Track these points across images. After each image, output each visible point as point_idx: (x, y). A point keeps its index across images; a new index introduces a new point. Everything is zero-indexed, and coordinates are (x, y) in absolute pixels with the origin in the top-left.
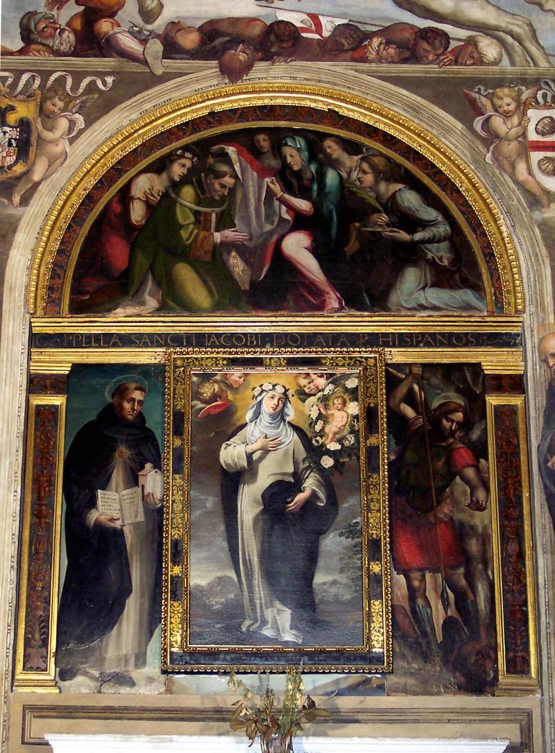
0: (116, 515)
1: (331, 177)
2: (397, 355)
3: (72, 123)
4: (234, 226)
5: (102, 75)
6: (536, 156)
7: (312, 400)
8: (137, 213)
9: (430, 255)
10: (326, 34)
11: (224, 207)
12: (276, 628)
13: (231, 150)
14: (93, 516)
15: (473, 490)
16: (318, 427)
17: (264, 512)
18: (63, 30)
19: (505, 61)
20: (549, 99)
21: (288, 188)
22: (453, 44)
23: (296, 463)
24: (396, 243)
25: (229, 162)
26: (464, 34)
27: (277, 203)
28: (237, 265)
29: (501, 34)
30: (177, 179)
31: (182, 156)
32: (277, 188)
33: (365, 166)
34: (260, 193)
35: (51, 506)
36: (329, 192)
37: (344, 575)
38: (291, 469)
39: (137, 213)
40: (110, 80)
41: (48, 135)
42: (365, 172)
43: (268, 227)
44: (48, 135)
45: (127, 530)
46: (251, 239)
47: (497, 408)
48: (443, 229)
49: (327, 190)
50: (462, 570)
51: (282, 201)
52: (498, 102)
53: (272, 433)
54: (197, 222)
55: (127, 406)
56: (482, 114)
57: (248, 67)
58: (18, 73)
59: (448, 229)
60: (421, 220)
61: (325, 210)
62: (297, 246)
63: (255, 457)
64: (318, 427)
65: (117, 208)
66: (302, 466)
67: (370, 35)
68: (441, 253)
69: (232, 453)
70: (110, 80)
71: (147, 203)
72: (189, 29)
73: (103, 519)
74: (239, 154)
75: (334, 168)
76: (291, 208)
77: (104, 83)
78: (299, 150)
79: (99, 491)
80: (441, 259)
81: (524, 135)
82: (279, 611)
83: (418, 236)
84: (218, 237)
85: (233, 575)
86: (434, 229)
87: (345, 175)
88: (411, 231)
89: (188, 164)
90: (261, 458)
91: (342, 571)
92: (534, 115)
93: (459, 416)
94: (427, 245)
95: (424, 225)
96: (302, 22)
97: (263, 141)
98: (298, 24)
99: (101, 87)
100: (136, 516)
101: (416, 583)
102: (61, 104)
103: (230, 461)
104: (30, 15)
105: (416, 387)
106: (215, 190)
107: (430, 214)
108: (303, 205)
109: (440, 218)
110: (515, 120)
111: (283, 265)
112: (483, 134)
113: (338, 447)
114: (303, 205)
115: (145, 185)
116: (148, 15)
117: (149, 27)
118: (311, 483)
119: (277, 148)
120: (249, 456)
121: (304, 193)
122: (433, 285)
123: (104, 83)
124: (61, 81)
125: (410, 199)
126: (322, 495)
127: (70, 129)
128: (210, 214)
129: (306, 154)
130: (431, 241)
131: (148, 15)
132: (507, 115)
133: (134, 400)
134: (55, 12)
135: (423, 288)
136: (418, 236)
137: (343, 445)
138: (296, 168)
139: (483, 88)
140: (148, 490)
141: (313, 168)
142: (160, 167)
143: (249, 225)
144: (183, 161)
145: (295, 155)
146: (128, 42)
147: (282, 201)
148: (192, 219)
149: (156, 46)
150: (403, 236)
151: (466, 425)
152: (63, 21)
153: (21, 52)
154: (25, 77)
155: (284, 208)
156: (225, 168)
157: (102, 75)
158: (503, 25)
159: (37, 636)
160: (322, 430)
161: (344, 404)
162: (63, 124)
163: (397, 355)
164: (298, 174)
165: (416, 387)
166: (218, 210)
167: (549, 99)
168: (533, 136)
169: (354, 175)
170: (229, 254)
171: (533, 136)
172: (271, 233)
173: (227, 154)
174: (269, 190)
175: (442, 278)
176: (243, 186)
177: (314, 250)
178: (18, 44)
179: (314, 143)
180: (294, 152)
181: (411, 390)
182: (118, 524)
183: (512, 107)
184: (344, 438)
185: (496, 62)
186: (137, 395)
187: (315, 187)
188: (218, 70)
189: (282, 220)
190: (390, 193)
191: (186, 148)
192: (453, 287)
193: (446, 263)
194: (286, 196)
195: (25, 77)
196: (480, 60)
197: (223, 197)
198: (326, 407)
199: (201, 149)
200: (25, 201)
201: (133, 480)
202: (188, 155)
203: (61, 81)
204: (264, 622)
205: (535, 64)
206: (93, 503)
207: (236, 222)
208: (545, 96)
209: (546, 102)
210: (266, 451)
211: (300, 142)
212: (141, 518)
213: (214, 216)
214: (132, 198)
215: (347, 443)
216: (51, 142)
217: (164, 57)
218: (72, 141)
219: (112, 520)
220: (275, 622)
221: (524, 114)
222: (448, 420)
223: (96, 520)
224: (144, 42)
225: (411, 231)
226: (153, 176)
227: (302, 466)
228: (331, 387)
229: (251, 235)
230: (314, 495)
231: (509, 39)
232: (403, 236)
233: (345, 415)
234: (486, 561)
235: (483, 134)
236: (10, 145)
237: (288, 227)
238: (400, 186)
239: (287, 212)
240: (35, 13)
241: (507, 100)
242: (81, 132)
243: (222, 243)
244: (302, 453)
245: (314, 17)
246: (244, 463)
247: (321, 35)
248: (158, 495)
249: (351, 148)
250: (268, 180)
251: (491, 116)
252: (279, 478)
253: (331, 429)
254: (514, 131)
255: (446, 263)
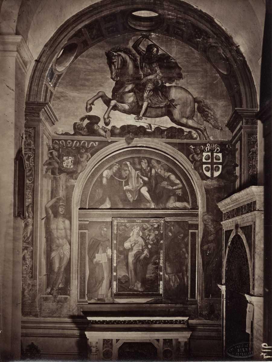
0: (100, 260)
1: (153, 171)
2: (168, 219)
3: (88, 156)
4: (129, 185)
5: (95, 141)
6: (204, 166)
7: (146, 231)
8: (105, 181)
9: (177, 193)
10: (153, 130)
11: (126, 179)
12: (137, 287)
13: (128, 163)
14: (95, 260)
15: (185, 254)
16: (148, 238)
17: (134, 259)
18: (84, 128)
19: (198, 139)
20: (209, 150)
21: (142, 174)
22: (185, 133)
23: (142, 247)
24: (169, 190)
25: (128, 167)
26: (188, 130)
27: (139, 178)
28: (129, 196)
29: (198, 130)
30: (114, 171)
31: (116, 165)
32: (140, 174)
33: (162, 168)
34: (135, 176)
35: (85, 258)
36: (153, 176)
37: (153, 274)
38: (141, 248)
39: (105, 181)
40: (97, 143)
41: (82, 160)
42: (162, 170)
43: (137, 185)
44: (82, 160)
45: (103, 264)
46: (133, 189)
47: (192, 233)
48: (180, 186)
49: (152, 175)
50: (181, 274)
51: (141, 178)
52: (196, 150)
53: (136, 239)
54: (119, 184)
55: (103, 232)
56: (192, 154)
57: (133, 139)
58: (73, 141)
59: (182, 185)
60: (176, 183)
61: (151, 181)
62: (144, 191)
63: (133, 245)
64: (148, 238)
65: (99, 179)
66: (144, 247)
67: (164, 131)
68: (179, 192)
69: (127, 245)
70: (97, 143)
71: (107, 178)
72: (118, 129)
73: (97, 261)
74: (131, 164)
75: (154, 168)
76: (143, 180)
77: (96, 144)
78: (145, 163)
79: (96, 254)
80: (179, 194)
81: (202, 160)
82: (138, 283)
83: (174, 188)
84: (125, 188)
85: (128, 275)
86: (178, 186)
87: (157, 170)
88: (173, 186)
89: (117, 167)
90: (134, 246)
91: (153, 273)
92: (205, 154)
93: (182, 235)
94: (177, 190)
95: (176, 184)
96: (147, 126)
97: (137, 160)
98: (146, 127)
99: (95, 145)
100: (105, 260)
101: (171, 277)
102: (84, 150)
103: (126, 246)
104: (75, 124)
105: (172, 228)
106: (124, 175)
107: (178, 181)
108: (146, 179)
109: (180, 183)
110: (200, 156)
111: (140, 195)
112: (191, 160)
113: (152, 242)
114: (146, 179)
115: (106, 173)
116: (107, 124)
117: (107, 127)
118: (146, 252)
119: (140, 164)
120: (131, 245)
121: (147, 176)
122: (177, 201)
123: (96, 144)
124: (84, 143)
125: (173, 177)
126: (148, 255)
127: (87, 158)
128: (123, 182)
129: (147, 164)
130: (177, 189)
131: (107, 124)
132: (198, 154)
133: (104, 230)
134: (82, 122)
135: (175, 202)
136: (174, 188)
137: (153, 242)
138: (144, 168)
139: (192, 146)
140: (108, 254)
141: (149, 168)
142: (110, 168)
143: (132, 184)
144: (116, 166)
145: (144, 165)
146: (102, 132)
147: (141, 178)
148: (118, 183)
149: (109, 133)
150: (170, 187)
151: (183, 238)
152: (84, 125)
153: (73, 135)
154: (75, 142)
155: (141, 180)
156: (127, 169)
157: (95, 141)
158: (198, 127)
159: (82, 290)
160: (149, 238)
161: (154, 231)
162: (85, 156)
163: (168, 219)
164: (144, 170)
165: (172, 228)
166: (125, 180)
167: (209, 150)
168: (204, 160)
169: (159, 170)
170: (128, 192)
171: (204, 160)
172: (138, 187)
173: (127, 164)
174: (138, 175)
175: (180, 199)
176: (131, 174)
177: (149, 191)
178: (72, 132)
179: (149, 161)
180: (144, 164)
181: (171, 228)
182: (101, 262)
183: (199, 152)
184: (154, 240)
185: (196, 139)
186: (105, 229)
187: (149, 174)
188: (125, 141)
189: (141, 183)
190: (168, 175)
191: (116, 163)
192: (182, 201)
193: (181, 195)
194: (142, 176)
195: (75, 142)
196: (191, 138)
197: (126, 177)
198: (150, 233)
199: (120, 163)
200: (76, 179)
201: (104, 252)
202: (117, 164)
203: (84, 143)
204: (134, 286)
205: (206, 139)
206: (95, 257)
207: (129, 184)
208: (208, 148)
209: (208, 150)
210: (135, 244)
211: (146, 161)
212: (106, 261)
213: (124, 182)
214: (103, 177)
215: (154, 242)
216: (82, 161)
217: (111, 136)
218: (88, 161)
219: (99, 261)
220: (137, 286)
221: (202, 154)
222: (180, 236)
223: (96, 262)
224: (106, 132)
225: (173, 186)
226: (108, 171)
227: (144, 247)
228: (151, 227)
229: (133, 186)
230: (146, 254)
231: (200, 132)
232: (170, 187)
233: (154, 234)
234: (187, 271)
235: (191, 160)
236: (72, 162)
237: (142, 185)
238: (170, 174)
239: (142, 181)
240: (76, 123)
241: (198, 150)
242: (90, 158)
243: (126, 189)
244: (144, 244)
245: (150, 125)
246: (130, 247)
247: (151, 130)
248: (111, 255)
249: (159, 162)
250: (138, 172)
251: (194, 155)
252: (138, 250)
253: (151, 237)
254: (199, 159)
255: (181, 195)
